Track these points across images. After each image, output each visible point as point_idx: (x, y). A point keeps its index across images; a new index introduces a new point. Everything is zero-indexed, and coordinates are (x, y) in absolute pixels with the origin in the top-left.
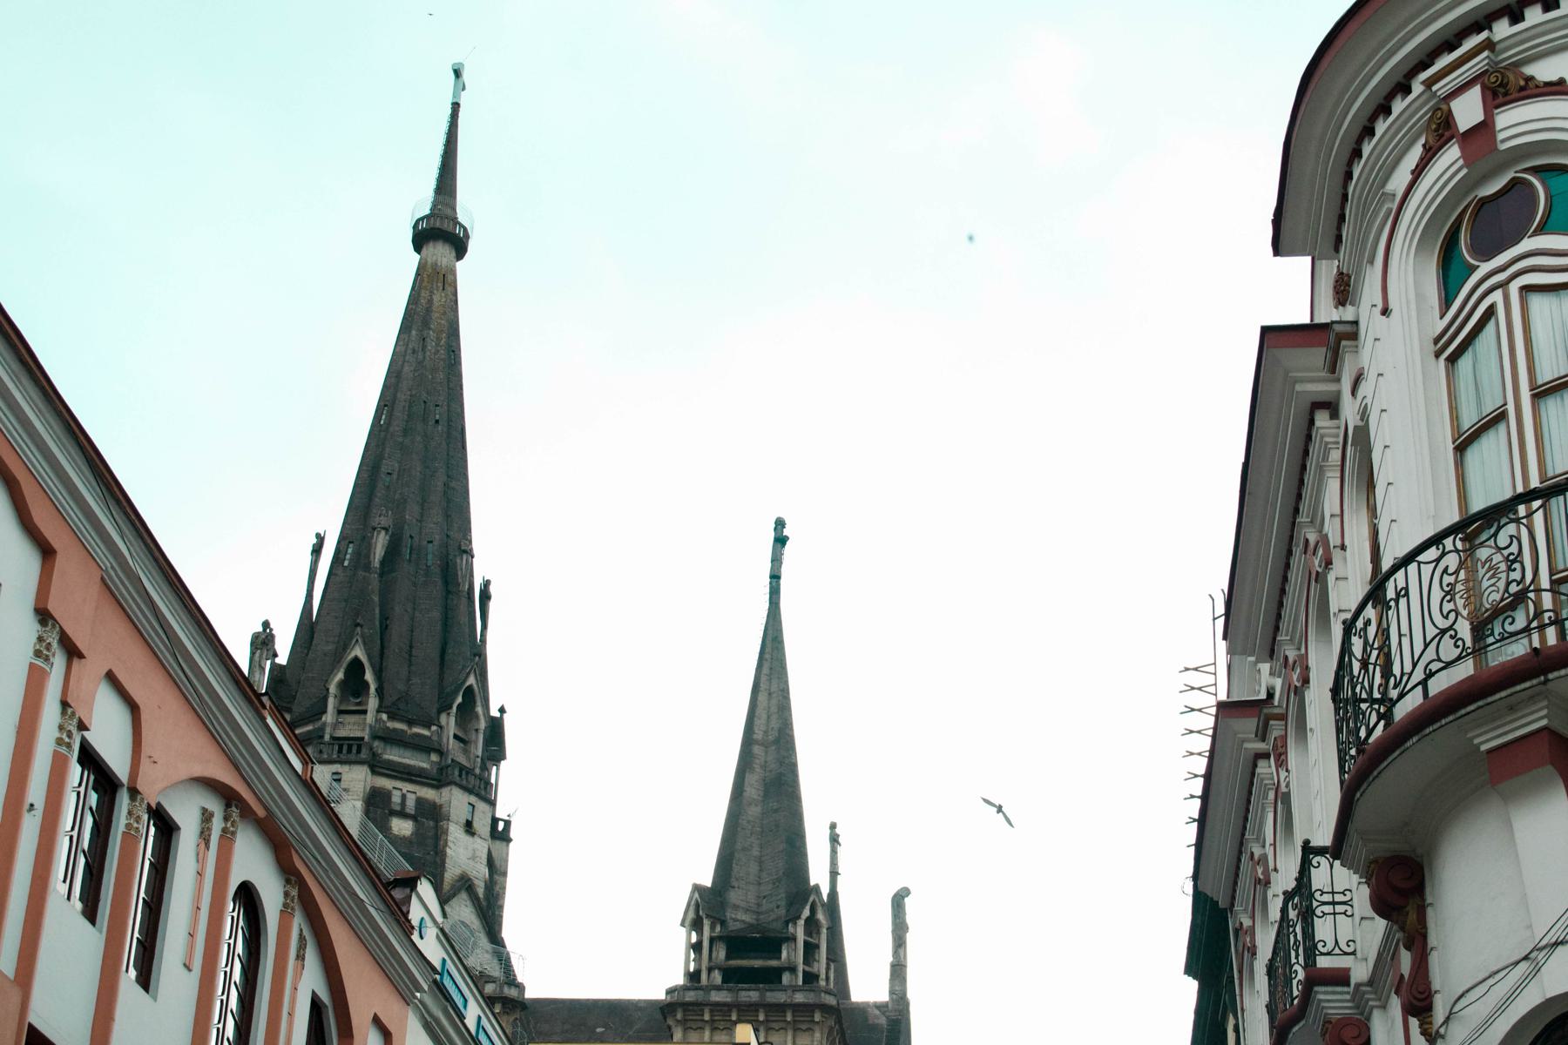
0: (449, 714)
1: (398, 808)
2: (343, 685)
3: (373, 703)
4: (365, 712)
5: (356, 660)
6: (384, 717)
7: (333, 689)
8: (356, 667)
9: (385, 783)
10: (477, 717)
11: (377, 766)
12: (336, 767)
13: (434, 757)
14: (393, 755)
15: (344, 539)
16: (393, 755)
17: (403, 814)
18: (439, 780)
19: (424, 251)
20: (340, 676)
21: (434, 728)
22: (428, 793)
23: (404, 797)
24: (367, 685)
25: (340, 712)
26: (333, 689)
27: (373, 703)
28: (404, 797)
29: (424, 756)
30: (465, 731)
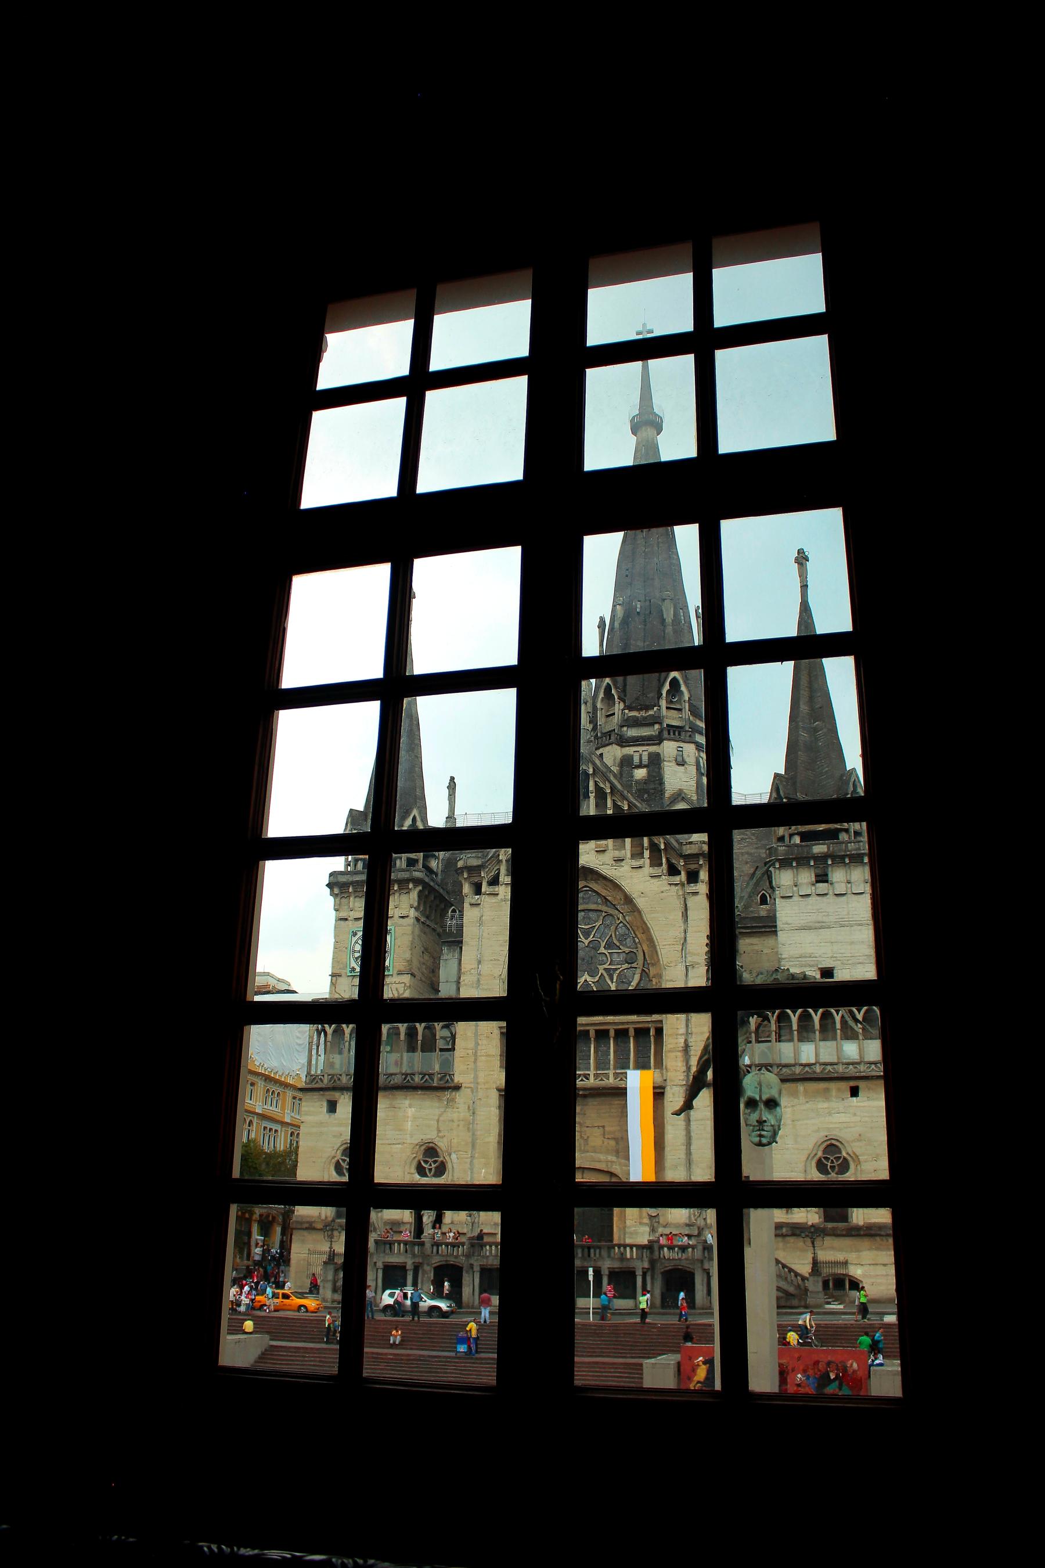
4: (614, 714)
5: (608, 683)
6: (627, 711)
9: (629, 750)
10: (682, 692)
14: (632, 732)
16: (632, 732)
17: (640, 766)
18: (658, 740)
19: (639, 434)
21: (655, 708)
22: (653, 749)
23: (641, 755)
25: (608, 716)
27: (619, 706)
28: (641, 755)
29: (651, 728)
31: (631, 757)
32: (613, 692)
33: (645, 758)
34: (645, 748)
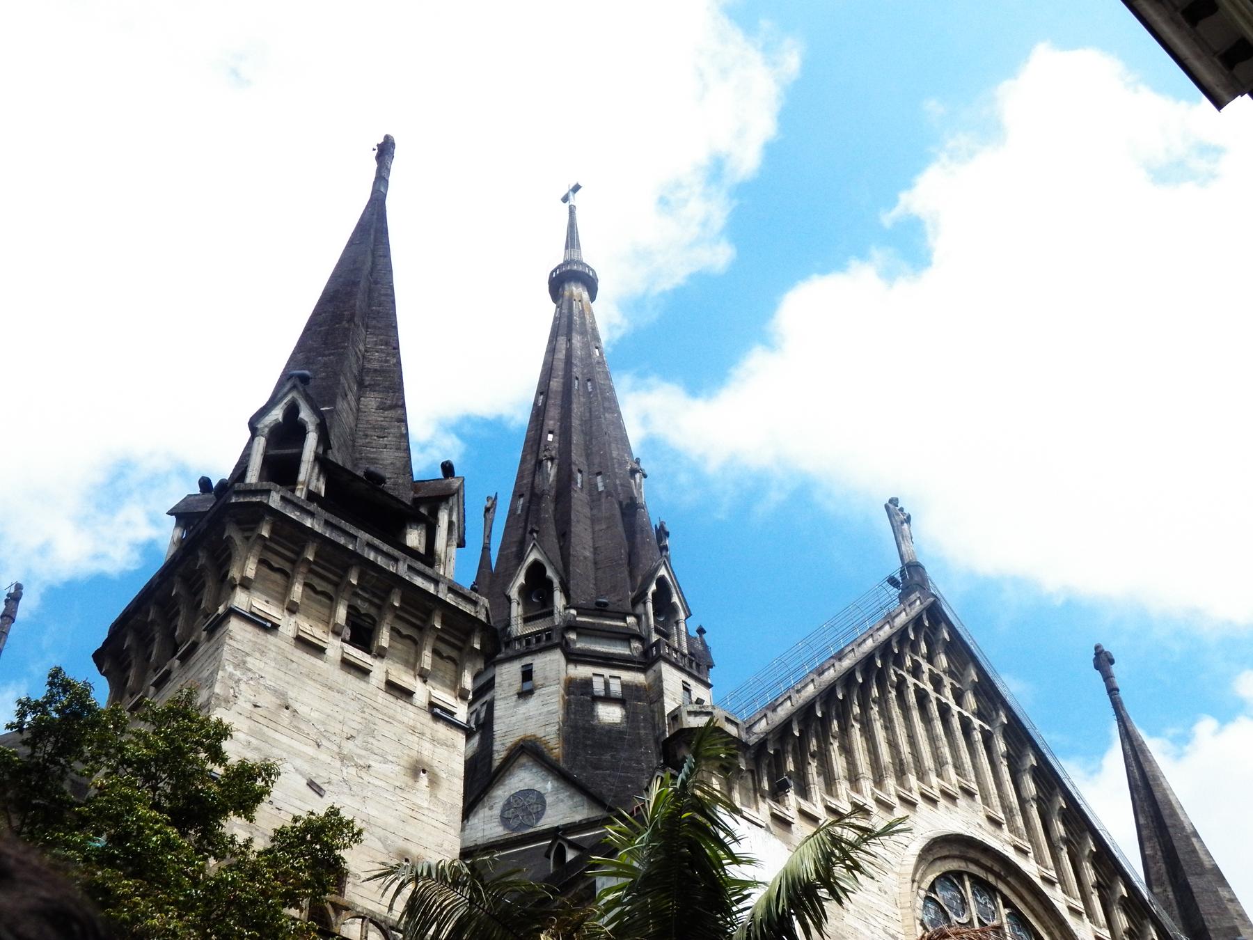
0: (645, 603)
1: (602, 694)
2: (523, 591)
3: (559, 600)
7: (514, 593)
8: (536, 571)
11: (574, 657)
12: (527, 660)
13: (636, 644)
15: (517, 494)
17: (608, 699)
20: (521, 580)
23: (607, 684)
24: (550, 582)
26: (514, 593)
28: (607, 684)
30: (665, 624)
31: (587, 683)
32: (550, 573)
33: (616, 688)
34: (616, 673)
